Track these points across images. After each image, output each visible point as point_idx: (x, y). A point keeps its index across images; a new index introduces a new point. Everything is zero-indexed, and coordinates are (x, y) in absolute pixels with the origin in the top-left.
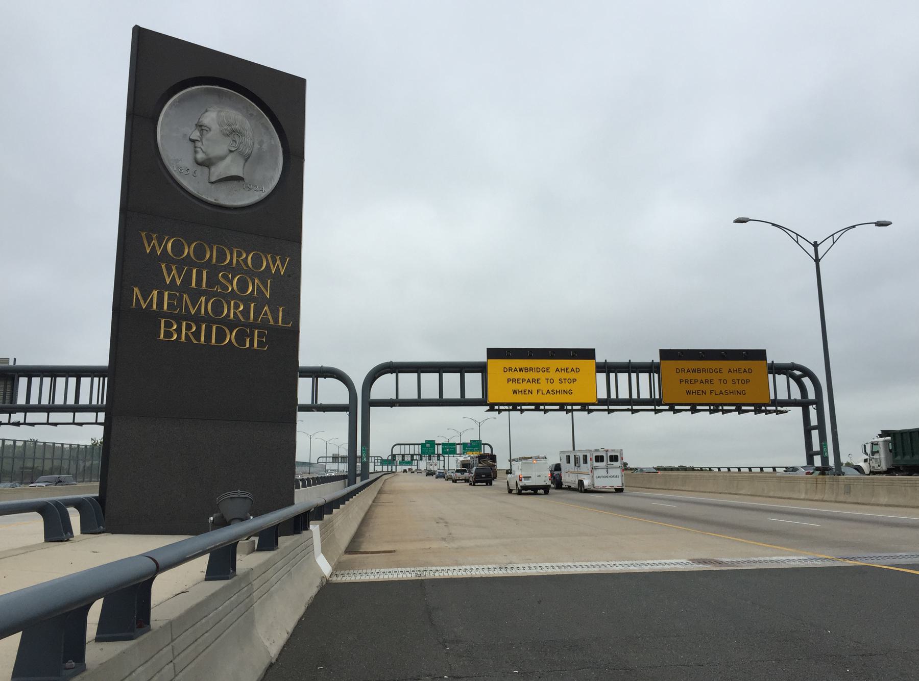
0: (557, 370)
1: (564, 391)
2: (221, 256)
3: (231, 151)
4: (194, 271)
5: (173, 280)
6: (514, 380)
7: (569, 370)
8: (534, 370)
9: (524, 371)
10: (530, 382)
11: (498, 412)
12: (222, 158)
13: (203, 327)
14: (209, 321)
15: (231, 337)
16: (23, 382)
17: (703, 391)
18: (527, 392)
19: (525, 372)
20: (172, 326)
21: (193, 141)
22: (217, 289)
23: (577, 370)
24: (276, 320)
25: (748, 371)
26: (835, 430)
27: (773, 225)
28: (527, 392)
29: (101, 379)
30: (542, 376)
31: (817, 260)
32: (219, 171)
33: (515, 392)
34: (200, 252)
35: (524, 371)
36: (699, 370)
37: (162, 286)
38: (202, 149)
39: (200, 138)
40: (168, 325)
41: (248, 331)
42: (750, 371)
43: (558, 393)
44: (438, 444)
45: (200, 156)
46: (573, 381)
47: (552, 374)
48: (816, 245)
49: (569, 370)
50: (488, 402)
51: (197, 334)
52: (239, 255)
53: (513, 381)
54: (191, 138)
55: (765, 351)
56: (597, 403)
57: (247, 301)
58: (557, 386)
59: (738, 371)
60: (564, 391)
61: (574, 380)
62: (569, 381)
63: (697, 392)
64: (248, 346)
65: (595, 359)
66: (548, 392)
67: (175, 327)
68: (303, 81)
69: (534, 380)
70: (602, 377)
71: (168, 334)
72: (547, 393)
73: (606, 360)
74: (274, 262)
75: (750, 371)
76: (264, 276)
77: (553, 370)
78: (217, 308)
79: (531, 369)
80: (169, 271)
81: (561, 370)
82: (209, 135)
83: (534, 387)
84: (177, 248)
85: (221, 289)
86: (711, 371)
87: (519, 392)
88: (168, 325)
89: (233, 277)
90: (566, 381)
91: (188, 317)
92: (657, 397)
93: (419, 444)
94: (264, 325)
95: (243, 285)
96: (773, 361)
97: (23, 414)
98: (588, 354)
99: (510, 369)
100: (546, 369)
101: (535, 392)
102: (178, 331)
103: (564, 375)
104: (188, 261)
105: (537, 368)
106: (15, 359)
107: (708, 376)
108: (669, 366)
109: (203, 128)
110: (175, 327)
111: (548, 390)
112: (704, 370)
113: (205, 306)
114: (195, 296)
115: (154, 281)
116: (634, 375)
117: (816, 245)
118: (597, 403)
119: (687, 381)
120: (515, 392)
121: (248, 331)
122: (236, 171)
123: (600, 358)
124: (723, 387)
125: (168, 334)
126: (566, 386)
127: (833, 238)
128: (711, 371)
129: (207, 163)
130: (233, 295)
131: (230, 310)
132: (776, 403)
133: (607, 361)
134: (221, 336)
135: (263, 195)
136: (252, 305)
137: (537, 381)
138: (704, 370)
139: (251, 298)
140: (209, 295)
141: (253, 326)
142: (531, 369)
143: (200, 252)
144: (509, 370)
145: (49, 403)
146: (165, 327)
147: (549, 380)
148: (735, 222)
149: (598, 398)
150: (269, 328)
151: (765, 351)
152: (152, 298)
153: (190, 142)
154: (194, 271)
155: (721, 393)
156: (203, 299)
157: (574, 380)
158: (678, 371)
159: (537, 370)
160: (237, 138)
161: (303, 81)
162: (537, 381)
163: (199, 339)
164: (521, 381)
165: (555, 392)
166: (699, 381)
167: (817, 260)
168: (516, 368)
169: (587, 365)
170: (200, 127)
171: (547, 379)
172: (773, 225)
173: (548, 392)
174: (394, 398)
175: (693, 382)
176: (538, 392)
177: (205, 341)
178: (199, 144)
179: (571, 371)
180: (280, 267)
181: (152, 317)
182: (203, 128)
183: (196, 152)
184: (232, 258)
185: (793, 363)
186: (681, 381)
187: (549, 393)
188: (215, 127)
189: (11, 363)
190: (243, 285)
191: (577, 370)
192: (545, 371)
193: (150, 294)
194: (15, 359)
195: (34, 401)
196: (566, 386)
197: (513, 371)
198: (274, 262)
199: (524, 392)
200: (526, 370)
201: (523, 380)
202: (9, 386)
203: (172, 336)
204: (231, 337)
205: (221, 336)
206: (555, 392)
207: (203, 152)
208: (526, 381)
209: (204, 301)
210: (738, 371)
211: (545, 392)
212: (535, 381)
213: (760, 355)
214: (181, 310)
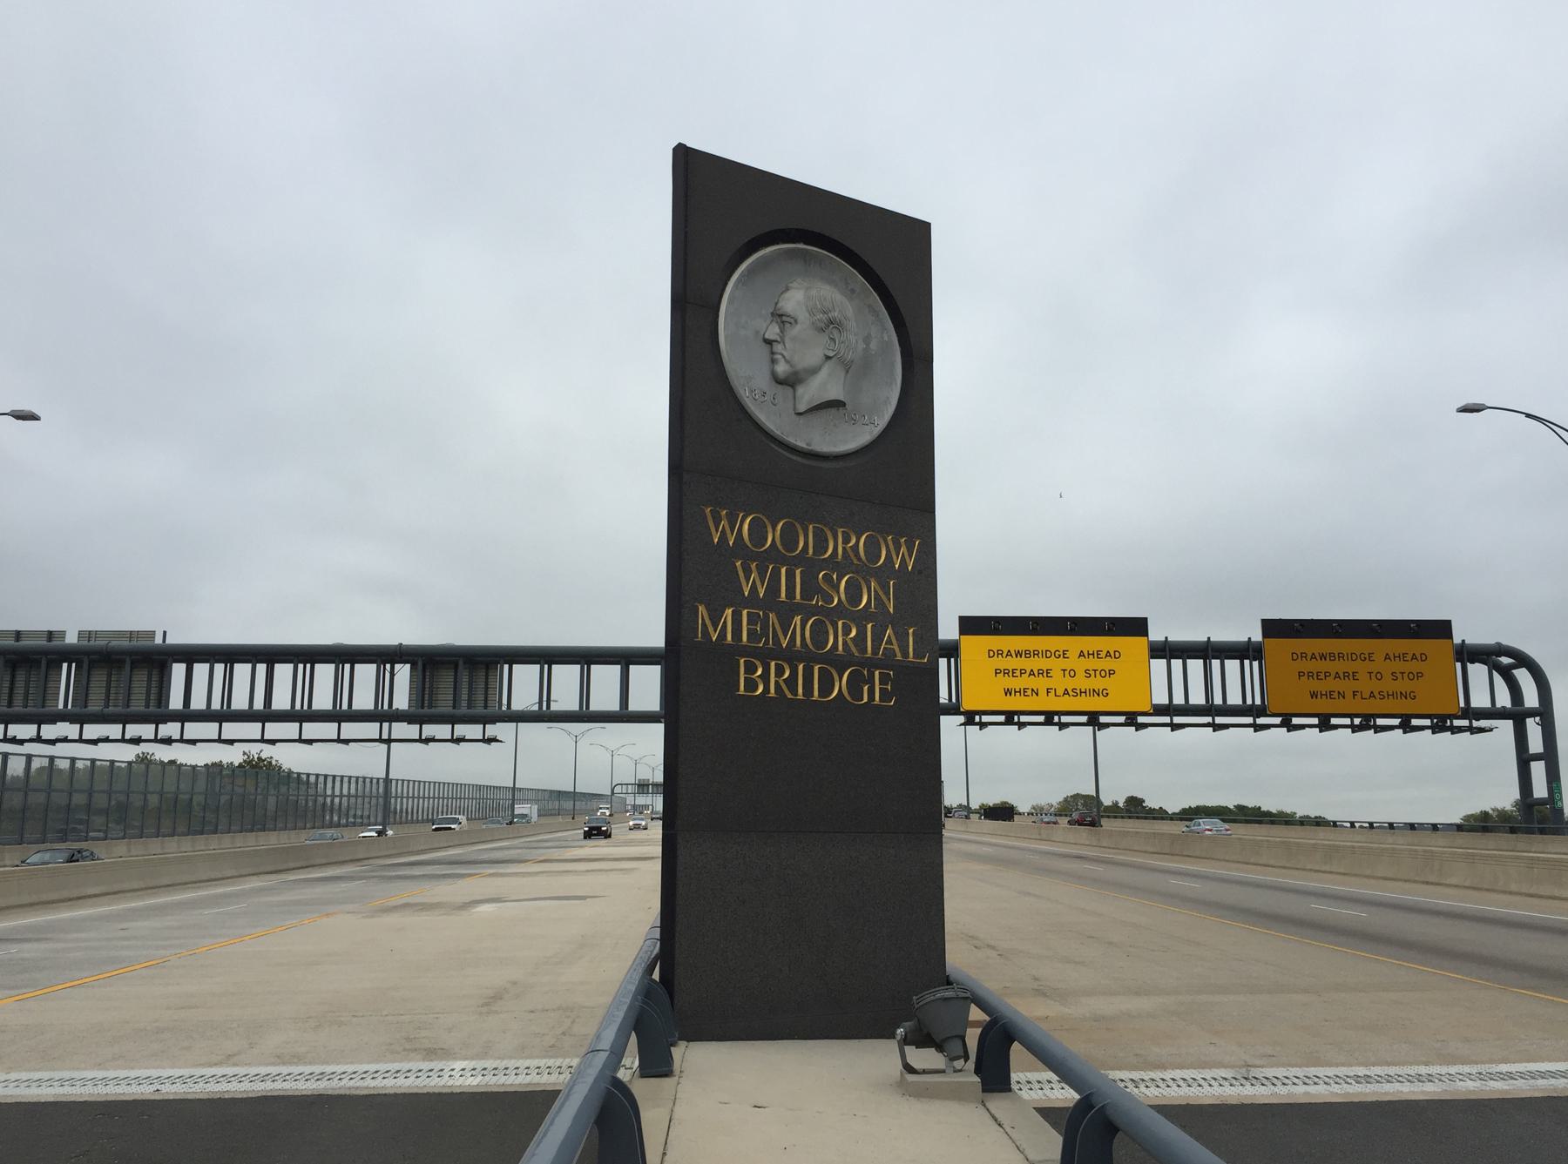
0: (1082, 654)
1: (1094, 690)
2: (821, 545)
3: (828, 358)
4: (783, 570)
5: (754, 589)
6: (1006, 672)
8: (1040, 655)
9: (1023, 655)
10: (1034, 674)
11: (978, 727)
12: (814, 371)
13: (801, 667)
14: (809, 658)
16: (179, 670)
18: (1029, 692)
20: (756, 671)
21: (769, 342)
22: (817, 602)
24: (905, 653)
27: (1528, 416)
28: (1029, 692)
29: (308, 666)
30: (1055, 664)
32: (810, 393)
33: (1008, 692)
34: (789, 539)
35: (1023, 655)
37: (739, 602)
38: (784, 357)
39: (781, 337)
40: (750, 669)
41: (866, 673)
42: (1423, 657)
43: (1083, 694)
45: (781, 368)
46: (1110, 674)
47: (1073, 662)
50: (962, 710)
51: (791, 682)
52: (846, 540)
53: (1004, 673)
54: (766, 336)
55: (1449, 622)
56: (1152, 711)
57: (861, 618)
58: (1081, 682)
59: (1402, 657)
60: (1094, 690)
61: (1111, 672)
62: (1103, 674)
64: (865, 700)
65: (1147, 635)
66: (1066, 692)
67: (759, 672)
68: (925, 228)
69: (1041, 672)
70: (1159, 665)
71: (751, 685)
72: (1064, 694)
73: (1166, 638)
75: (1424, 658)
77: (1073, 655)
78: (819, 634)
81: (1089, 654)
82: (794, 331)
83: (1041, 683)
84: (758, 532)
85: (823, 601)
86: (1353, 657)
87: (1015, 692)
88: (750, 669)
89: (840, 579)
90: (1098, 673)
92: (1258, 702)
94: (887, 662)
95: (854, 594)
96: (1463, 641)
97: (179, 724)
98: (1136, 627)
99: (1000, 653)
100: (1061, 653)
101: (1042, 692)
102: (765, 677)
104: (773, 556)
106: (165, 633)
107: (1350, 667)
108: (1280, 648)
109: (784, 318)
110: (759, 672)
111: (1066, 690)
112: (1341, 656)
113: (801, 631)
114: (786, 614)
115: (725, 594)
116: (1216, 663)
118: (1152, 711)
119: (1310, 675)
120: (1008, 692)
121: (866, 673)
122: (835, 392)
123: (1156, 634)
124: (1376, 686)
125: (751, 685)
126: (1097, 683)
128: (1353, 657)
129: (791, 382)
130: (840, 611)
131: (838, 639)
132: (1469, 713)
133: (1169, 639)
135: (877, 431)
136: (869, 626)
138: (1341, 656)
139: (866, 615)
140: (807, 612)
141: (872, 664)
143: (789, 539)
144: (998, 654)
145: (222, 706)
146: (745, 673)
147: (1067, 673)
148: (1461, 411)
149: (1153, 703)
151: (1449, 622)
152: (725, 622)
153: (764, 344)
154: (783, 570)
155: (1372, 695)
156: (798, 619)
159: (1047, 654)
160: (836, 335)
161: (925, 228)
163: (794, 691)
164: (1018, 673)
165: (1078, 693)
168: (1009, 651)
169: (1133, 646)
170: (780, 317)
171: (1064, 670)
172: (1528, 416)
173: (1066, 692)
176: (1048, 692)
177: (804, 695)
178: (778, 348)
179: (1106, 656)
180: (905, 558)
181: (725, 656)
182: (784, 318)
183: (773, 361)
184: (835, 546)
186: (1301, 674)
187: (1068, 694)
188: (802, 316)
189: (158, 640)
190: (854, 594)
191: (1115, 655)
192: (1060, 655)
193: (722, 616)
194: (165, 633)
195: (198, 703)
196: (1097, 683)
197: (1004, 655)
199: (1024, 692)
200: (1028, 654)
201: (1023, 672)
202: (155, 678)
203: (756, 689)
204: (841, 684)
206: (1078, 693)
207: (787, 361)
208: (1028, 673)
209: (799, 623)
210: (1402, 657)
211: (1060, 692)
212: (1042, 674)
213: (1442, 629)
214: (767, 642)
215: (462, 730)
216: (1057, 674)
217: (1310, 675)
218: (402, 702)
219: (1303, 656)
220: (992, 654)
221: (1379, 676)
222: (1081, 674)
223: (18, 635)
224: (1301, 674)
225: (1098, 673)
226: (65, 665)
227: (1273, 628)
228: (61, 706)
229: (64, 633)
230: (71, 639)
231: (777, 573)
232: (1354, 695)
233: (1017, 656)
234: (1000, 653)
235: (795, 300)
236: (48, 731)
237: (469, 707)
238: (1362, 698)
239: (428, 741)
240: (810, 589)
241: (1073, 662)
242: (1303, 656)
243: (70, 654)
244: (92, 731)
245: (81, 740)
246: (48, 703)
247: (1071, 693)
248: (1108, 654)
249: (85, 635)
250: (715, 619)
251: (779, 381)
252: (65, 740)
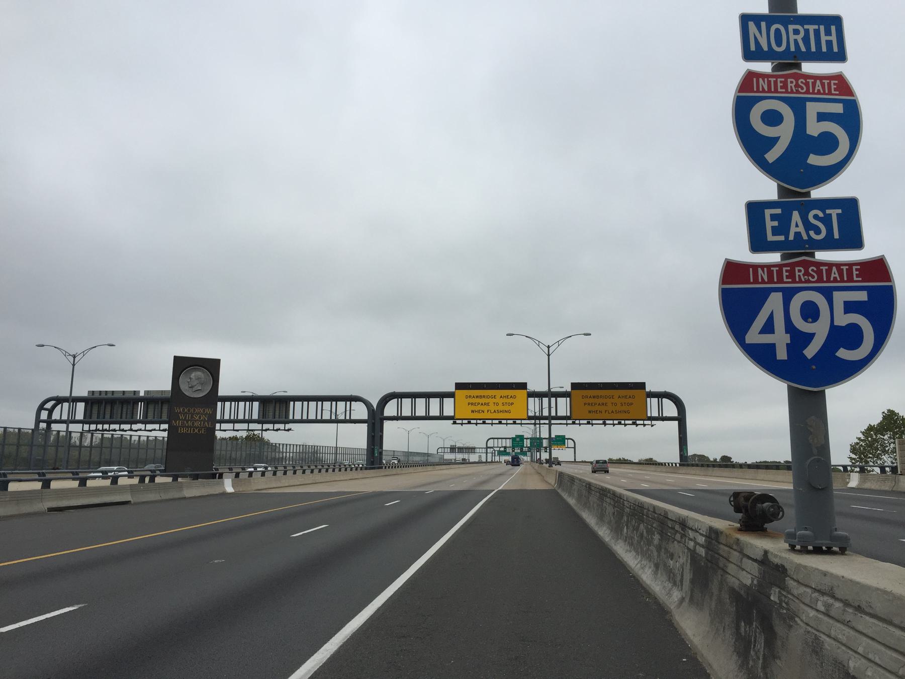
2: (195, 410)
6: (472, 404)
7: (509, 397)
12: (196, 385)
14: (191, 427)
15: (196, 431)
23: (514, 397)
24: (208, 425)
26: (681, 436)
27: (526, 337)
28: (481, 412)
30: (491, 401)
32: (195, 389)
33: (473, 411)
34: (189, 411)
36: (598, 397)
42: (634, 397)
44: (527, 439)
45: (190, 386)
47: (498, 400)
48: (549, 347)
49: (509, 397)
51: (188, 431)
57: (201, 421)
58: (501, 408)
61: (512, 404)
63: (596, 412)
66: (495, 411)
69: (485, 404)
74: (209, 410)
76: (205, 415)
77: (498, 397)
79: (484, 397)
80: (181, 416)
83: (485, 408)
86: (606, 397)
88: (181, 429)
91: (186, 427)
93: (510, 439)
95: (200, 417)
98: (523, 386)
99: (470, 396)
101: (486, 411)
103: (505, 400)
117: (549, 347)
119: (589, 404)
120: (473, 411)
128: (606, 397)
129: (192, 387)
130: (197, 420)
134: (194, 430)
137: (488, 404)
138: (601, 397)
140: (191, 421)
142: (484, 397)
143: (189, 411)
149: (529, 415)
150: (207, 428)
157: (512, 404)
159: (488, 397)
162: (488, 404)
165: (499, 412)
167: (549, 355)
169: (523, 393)
170: (190, 378)
171: (494, 403)
172: (526, 337)
173: (495, 411)
174: (396, 415)
181: (177, 428)
185: (665, 391)
186: (585, 404)
188: (194, 378)
190: (200, 417)
196: (507, 408)
198: (209, 410)
200: (481, 397)
201: (479, 404)
204: (196, 431)
205: (194, 430)
206: (499, 412)
213: (642, 386)
215: (277, 426)
216: (491, 404)
218: (255, 416)
219: (587, 397)
220: (467, 397)
221: (616, 404)
222: (500, 404)
223: (124, 392)
224: (585, 404)
226: (140, 403)
227: (575, 386)
228: (138, 418)
229: (139, 391)
230: (142, 394)
231: (186, 416)
232: (605, 412)
234: (470, 396)
235: (193, 375)
236: (135, 427)
237: (279, 418)
239: (277, 430)
240: (192, 417)
241: (498, 400)
242: (587, 397)
243: (141, 399)
244: (149, 427)
245: (145, 430)
246: (134, 417)
248: (511, 397)
249: (147, 392)
250: (176, 422)
251: (190, 387)
252: (141, 430)
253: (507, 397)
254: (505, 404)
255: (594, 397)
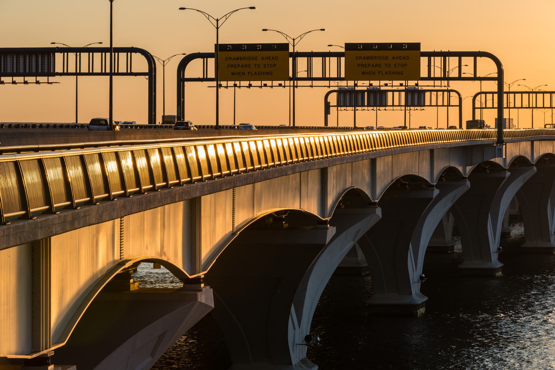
7: (271, 58)
9: (239, 59)
17: (373, 72)
18: (241, 74)
19: (240, 60)
25: (406, 58)
31: (217, 28)
43: (263, 74)
48: (217, 20)
62: (271, 66)
69: (246, 66)
87: (236, 74)
100: (255, 58)
105: (249, 57)
117: (217, 20)
127: (226, 16)
138: (375, 58)
158: (357, 58)
166: (372, 65)
167: (217, 28)
171: (255, 65)
175: (367, 66)
179: (272, 59)
187: (256, 74)
191: (276, 58)
197: (232, 59)
208: (241, 66)
217: (362, 65)
225: (269, 65)
233: (237, 60)
238: (382, 74)
247: (258, 74)
253: (269, 58)
254: (267, 66)
255: (368, 58)
